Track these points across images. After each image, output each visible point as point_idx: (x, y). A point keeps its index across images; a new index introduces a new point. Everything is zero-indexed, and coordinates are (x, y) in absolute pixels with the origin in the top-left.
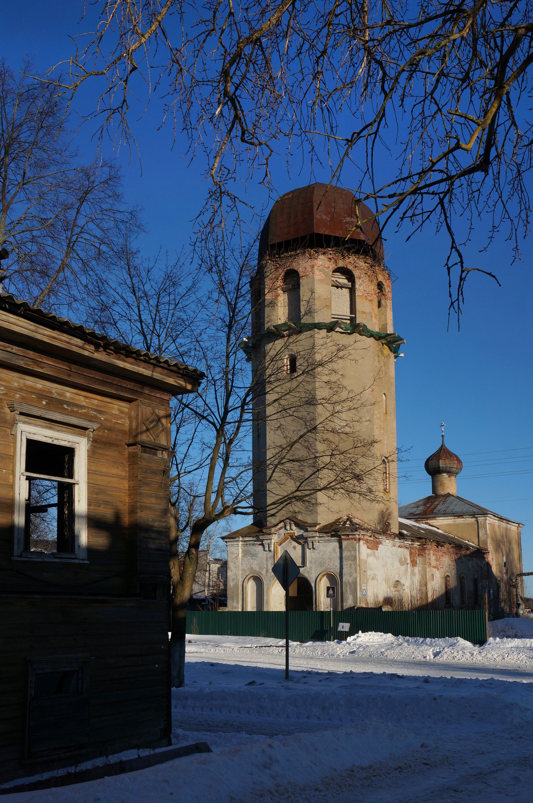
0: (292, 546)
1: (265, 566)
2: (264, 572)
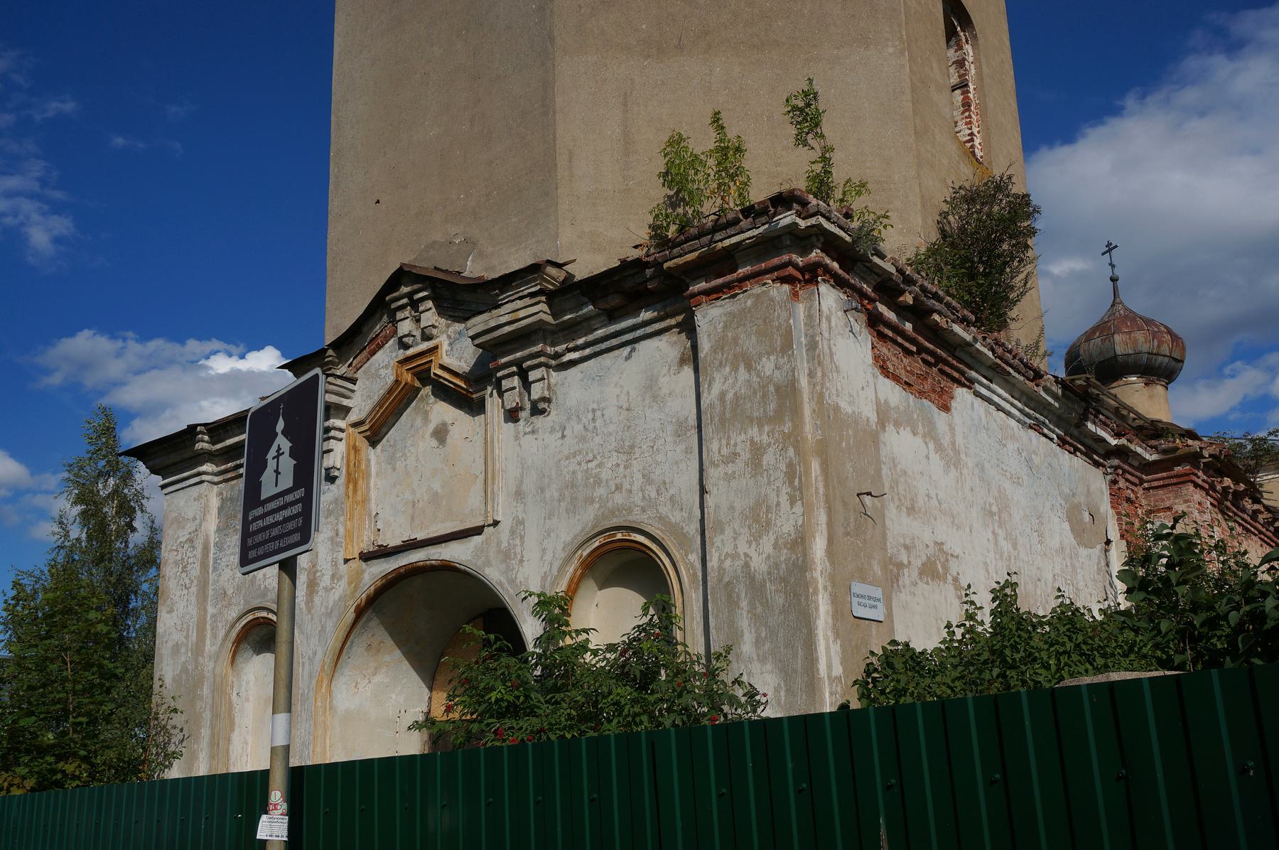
0: (431, 427)
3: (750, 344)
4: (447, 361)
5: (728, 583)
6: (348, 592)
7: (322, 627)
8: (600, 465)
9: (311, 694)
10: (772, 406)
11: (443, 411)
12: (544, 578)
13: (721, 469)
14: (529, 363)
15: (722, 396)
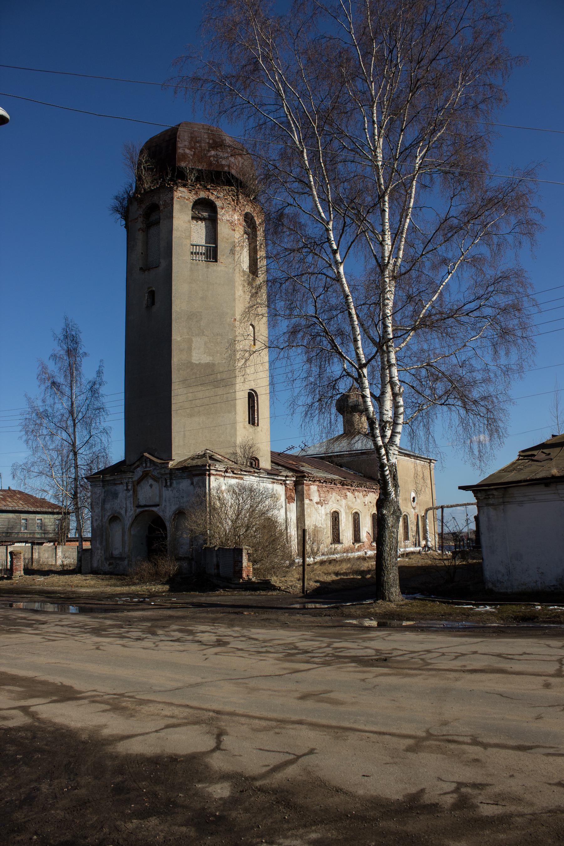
1: (125, 506)
2: (123, 512)
11: (151, 481)
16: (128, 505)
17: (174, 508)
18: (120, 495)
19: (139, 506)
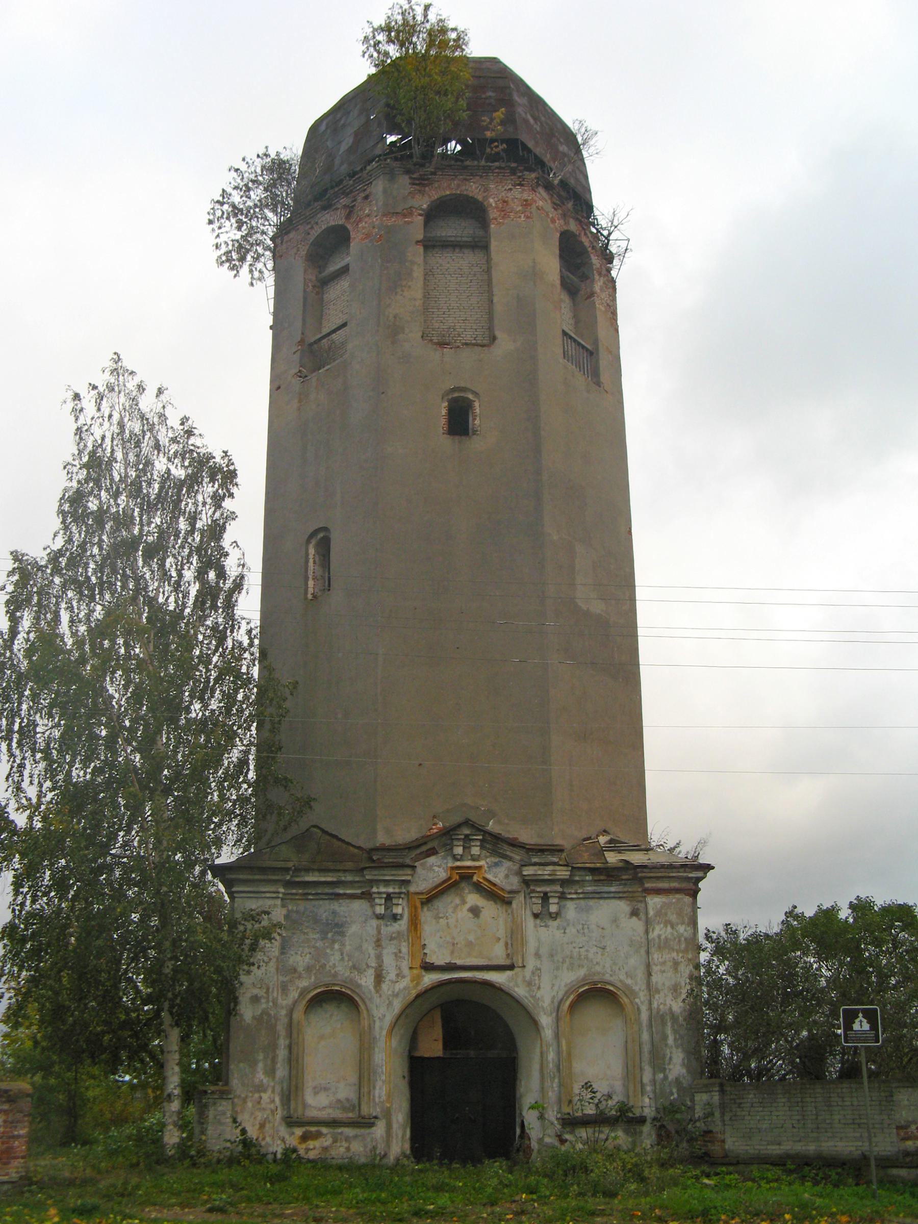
0: (468, 906)
2: (367, 981)
3: (673, 918)
4: (490, 876)
5: (662, 1015)
6: (411, 985)
7: (390, 1002)
8: (587, 951)
9: (383, 1039)
10: (683, 946)
11: (473, 899)
12: (554, 997)
13: (659, 967)
14: (552, 894)
15: (659, 936)
16: (389, 961)
17: (569, 977)
18: (354, 929)
19: (429, 967)
